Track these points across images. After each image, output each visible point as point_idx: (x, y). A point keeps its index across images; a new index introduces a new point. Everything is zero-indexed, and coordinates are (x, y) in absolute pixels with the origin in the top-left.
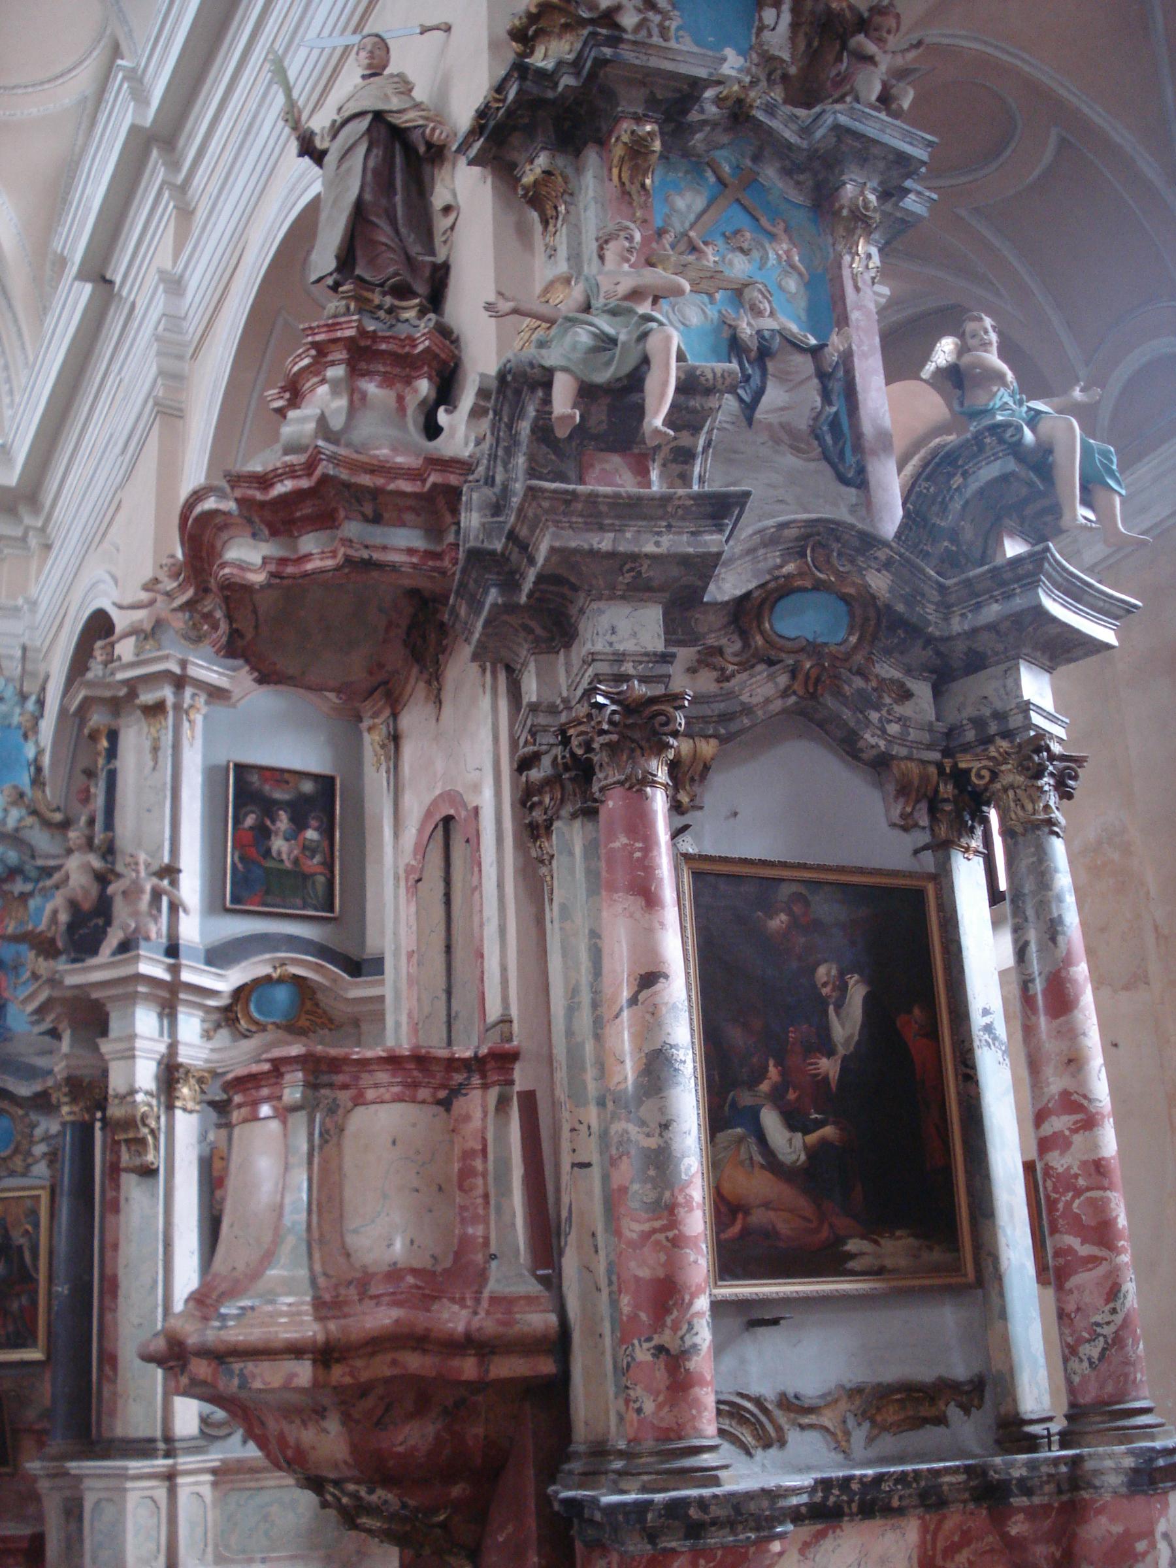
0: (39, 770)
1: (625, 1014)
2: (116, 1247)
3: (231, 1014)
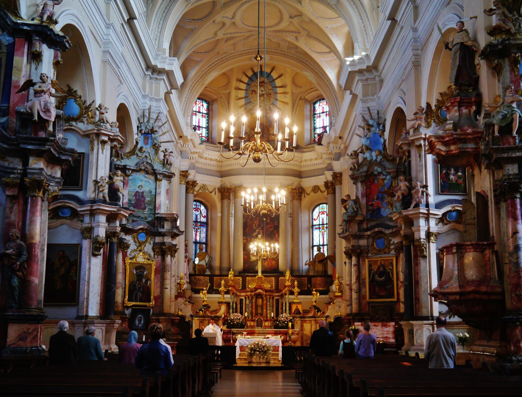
1: (511, 239)
2: (418, 274)
3: (442, 220)
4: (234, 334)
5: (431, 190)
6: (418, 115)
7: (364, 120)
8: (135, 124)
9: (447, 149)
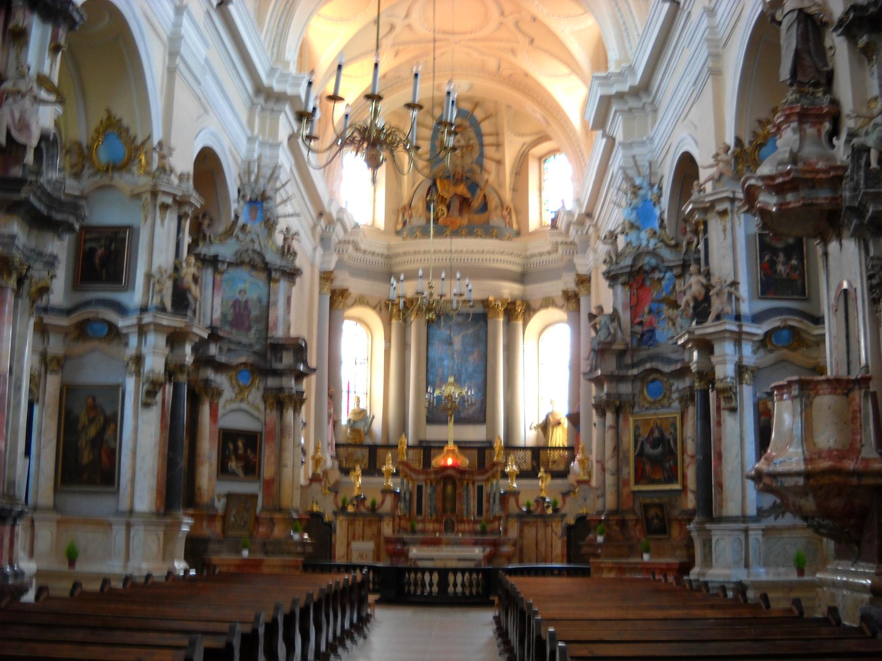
0: (662, 221)
3: (765, 343)
4: (404, 543)
5: (744, 290)
6: (719, 158)
7: (627, 178)
8: (232, 185)
9: (781, 201)
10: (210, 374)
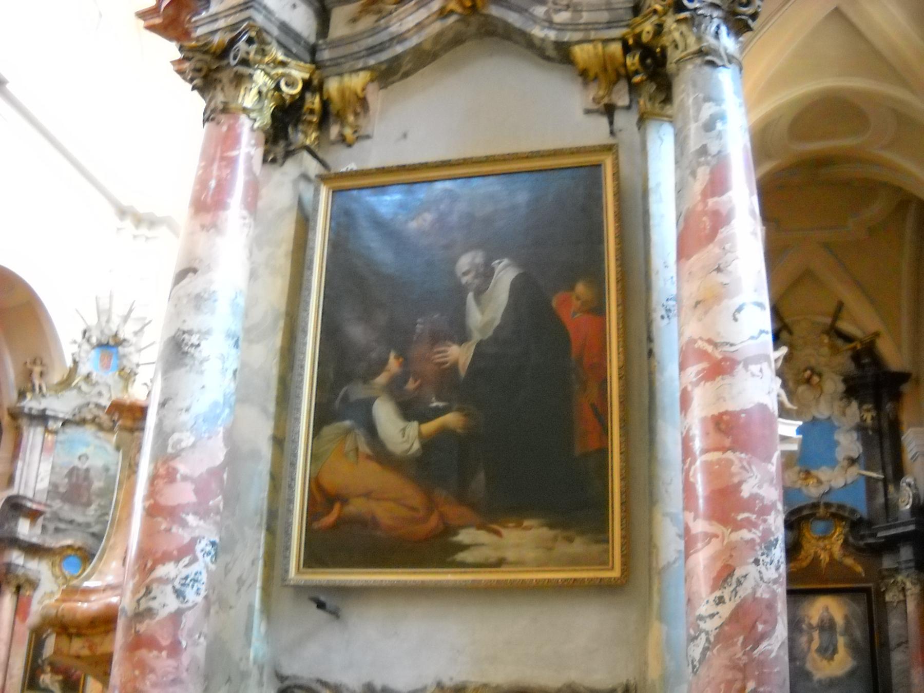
10: (17, 557)
